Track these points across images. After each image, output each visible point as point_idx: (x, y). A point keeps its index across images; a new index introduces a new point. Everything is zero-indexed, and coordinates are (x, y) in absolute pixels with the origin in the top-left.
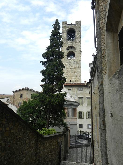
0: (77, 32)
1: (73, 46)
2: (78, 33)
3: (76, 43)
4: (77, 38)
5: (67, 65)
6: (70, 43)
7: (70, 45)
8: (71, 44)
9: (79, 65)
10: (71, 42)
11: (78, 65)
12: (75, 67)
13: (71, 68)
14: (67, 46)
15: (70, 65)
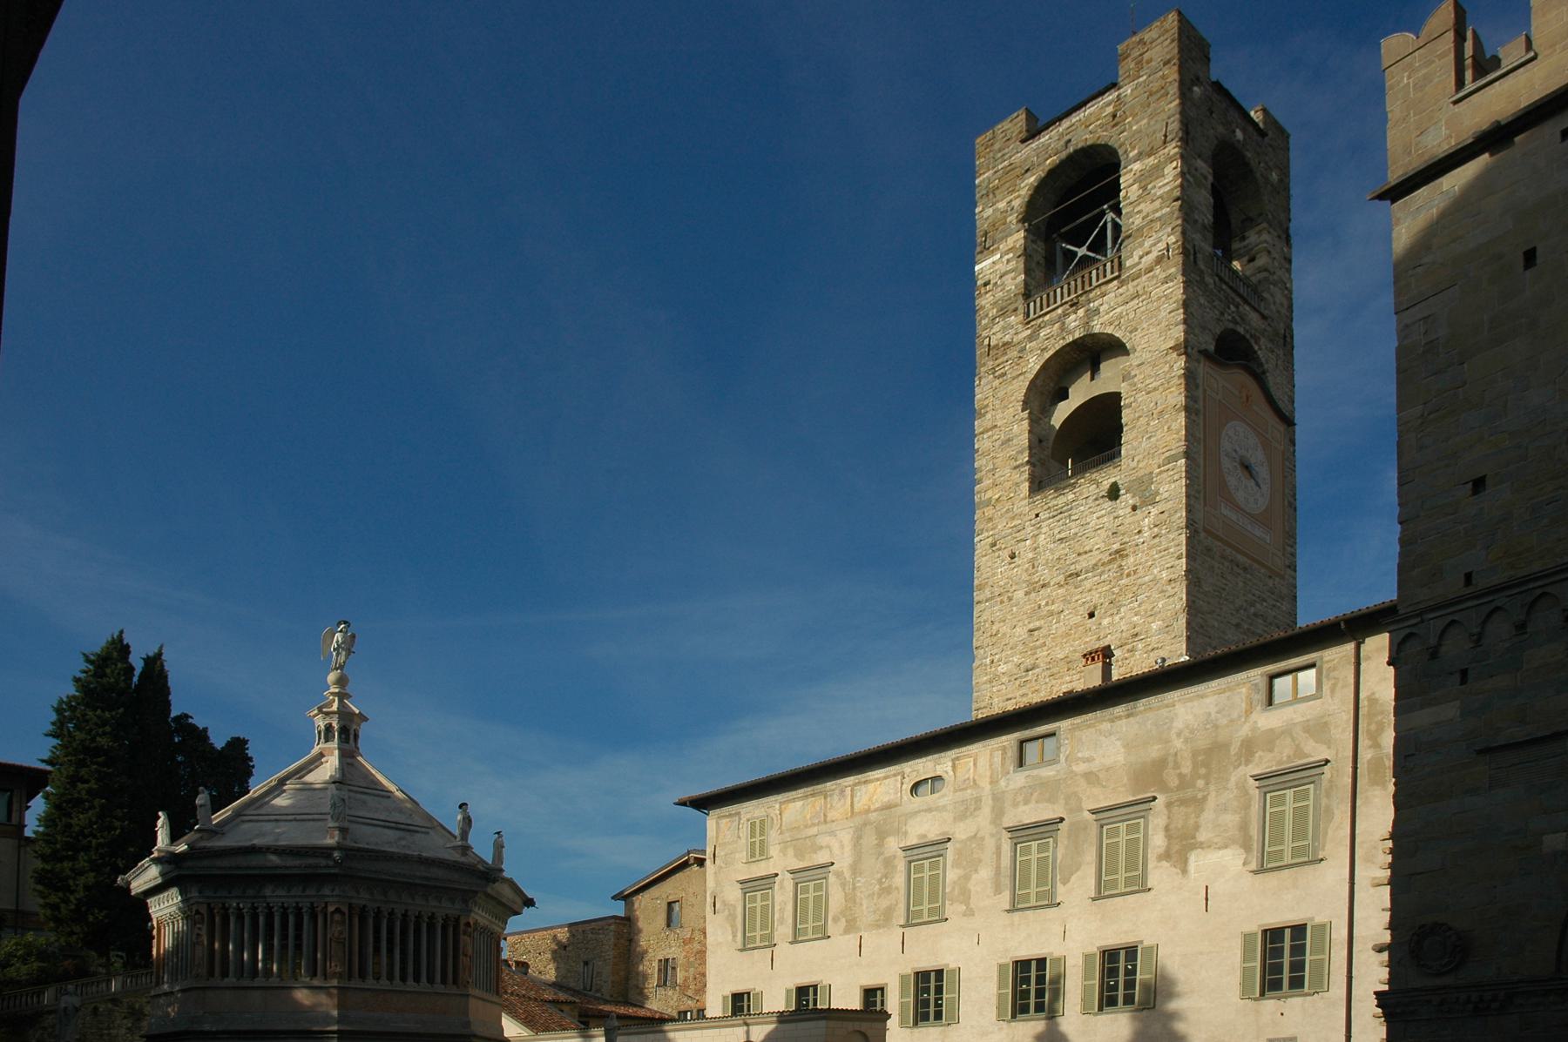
0: (1137, 166)
1: (1096, 330)
2: (1151, 161)
3: (1122, 283)
4: (1140, 229)
5: (1031, 555)
6: (1065, 315)
7: (1062, 343)
8: (1075, 325)
9: (1161, 507)
10: (1075, 305)
11: (1154, 511)
12: (1116, 547)
13: (1084, 562)
14: (1034, 364)
15: (1062, 550)
